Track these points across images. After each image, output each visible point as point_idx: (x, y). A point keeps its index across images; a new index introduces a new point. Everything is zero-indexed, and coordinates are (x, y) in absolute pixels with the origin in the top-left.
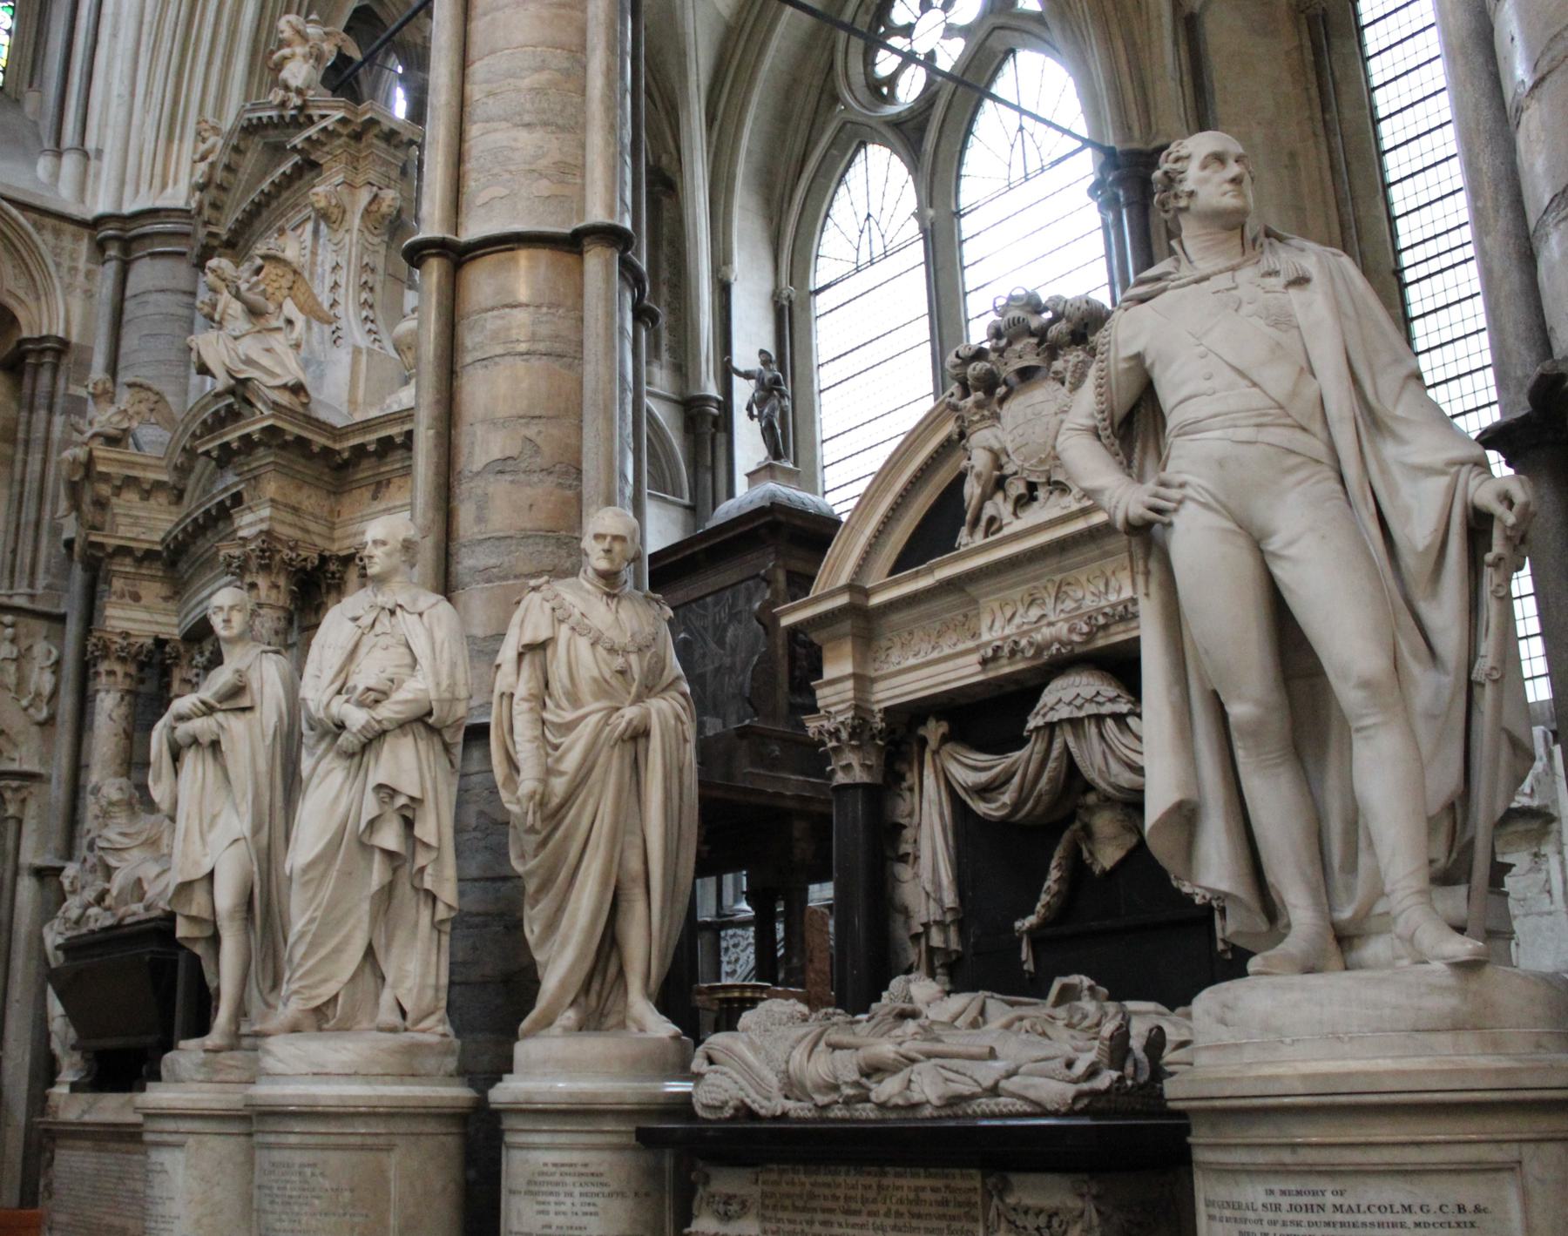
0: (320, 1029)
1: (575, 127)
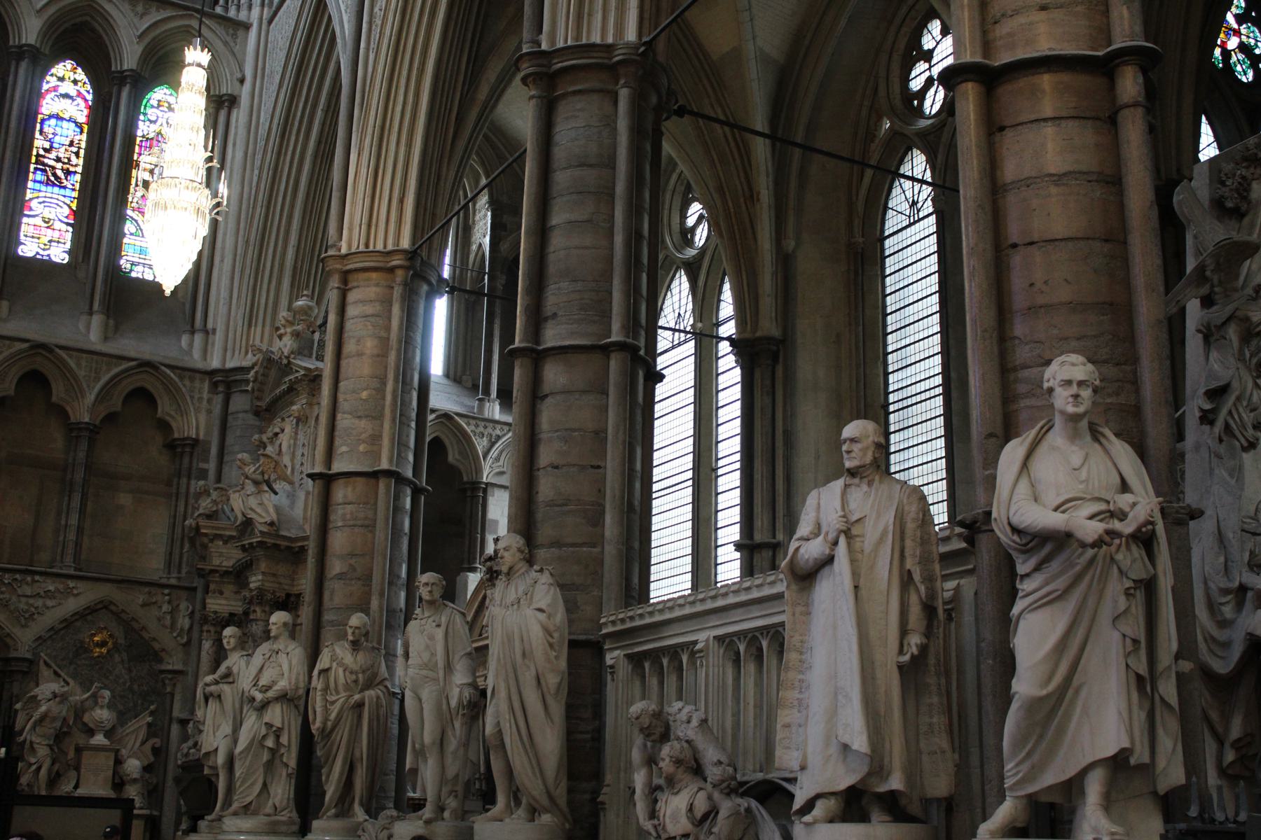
0: (246, 814)
1: (378, 417)
